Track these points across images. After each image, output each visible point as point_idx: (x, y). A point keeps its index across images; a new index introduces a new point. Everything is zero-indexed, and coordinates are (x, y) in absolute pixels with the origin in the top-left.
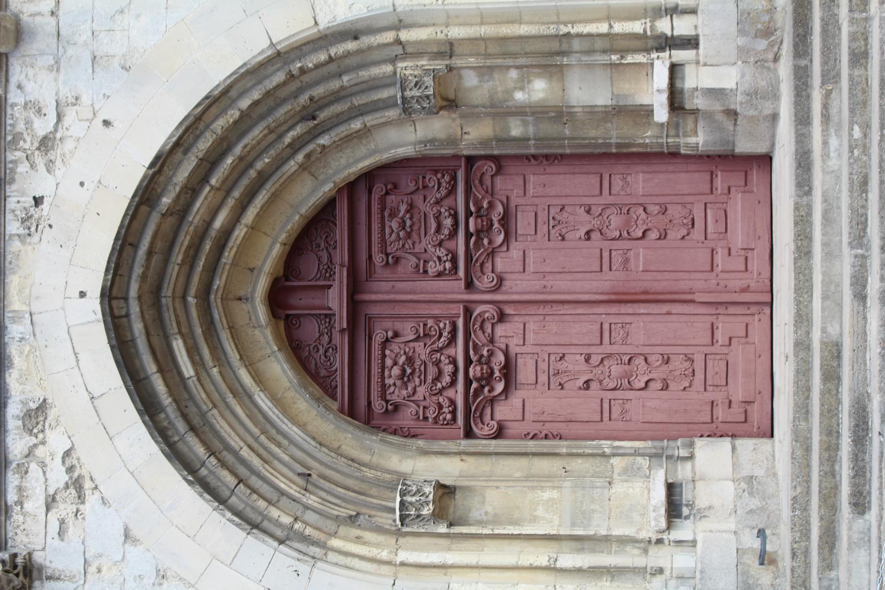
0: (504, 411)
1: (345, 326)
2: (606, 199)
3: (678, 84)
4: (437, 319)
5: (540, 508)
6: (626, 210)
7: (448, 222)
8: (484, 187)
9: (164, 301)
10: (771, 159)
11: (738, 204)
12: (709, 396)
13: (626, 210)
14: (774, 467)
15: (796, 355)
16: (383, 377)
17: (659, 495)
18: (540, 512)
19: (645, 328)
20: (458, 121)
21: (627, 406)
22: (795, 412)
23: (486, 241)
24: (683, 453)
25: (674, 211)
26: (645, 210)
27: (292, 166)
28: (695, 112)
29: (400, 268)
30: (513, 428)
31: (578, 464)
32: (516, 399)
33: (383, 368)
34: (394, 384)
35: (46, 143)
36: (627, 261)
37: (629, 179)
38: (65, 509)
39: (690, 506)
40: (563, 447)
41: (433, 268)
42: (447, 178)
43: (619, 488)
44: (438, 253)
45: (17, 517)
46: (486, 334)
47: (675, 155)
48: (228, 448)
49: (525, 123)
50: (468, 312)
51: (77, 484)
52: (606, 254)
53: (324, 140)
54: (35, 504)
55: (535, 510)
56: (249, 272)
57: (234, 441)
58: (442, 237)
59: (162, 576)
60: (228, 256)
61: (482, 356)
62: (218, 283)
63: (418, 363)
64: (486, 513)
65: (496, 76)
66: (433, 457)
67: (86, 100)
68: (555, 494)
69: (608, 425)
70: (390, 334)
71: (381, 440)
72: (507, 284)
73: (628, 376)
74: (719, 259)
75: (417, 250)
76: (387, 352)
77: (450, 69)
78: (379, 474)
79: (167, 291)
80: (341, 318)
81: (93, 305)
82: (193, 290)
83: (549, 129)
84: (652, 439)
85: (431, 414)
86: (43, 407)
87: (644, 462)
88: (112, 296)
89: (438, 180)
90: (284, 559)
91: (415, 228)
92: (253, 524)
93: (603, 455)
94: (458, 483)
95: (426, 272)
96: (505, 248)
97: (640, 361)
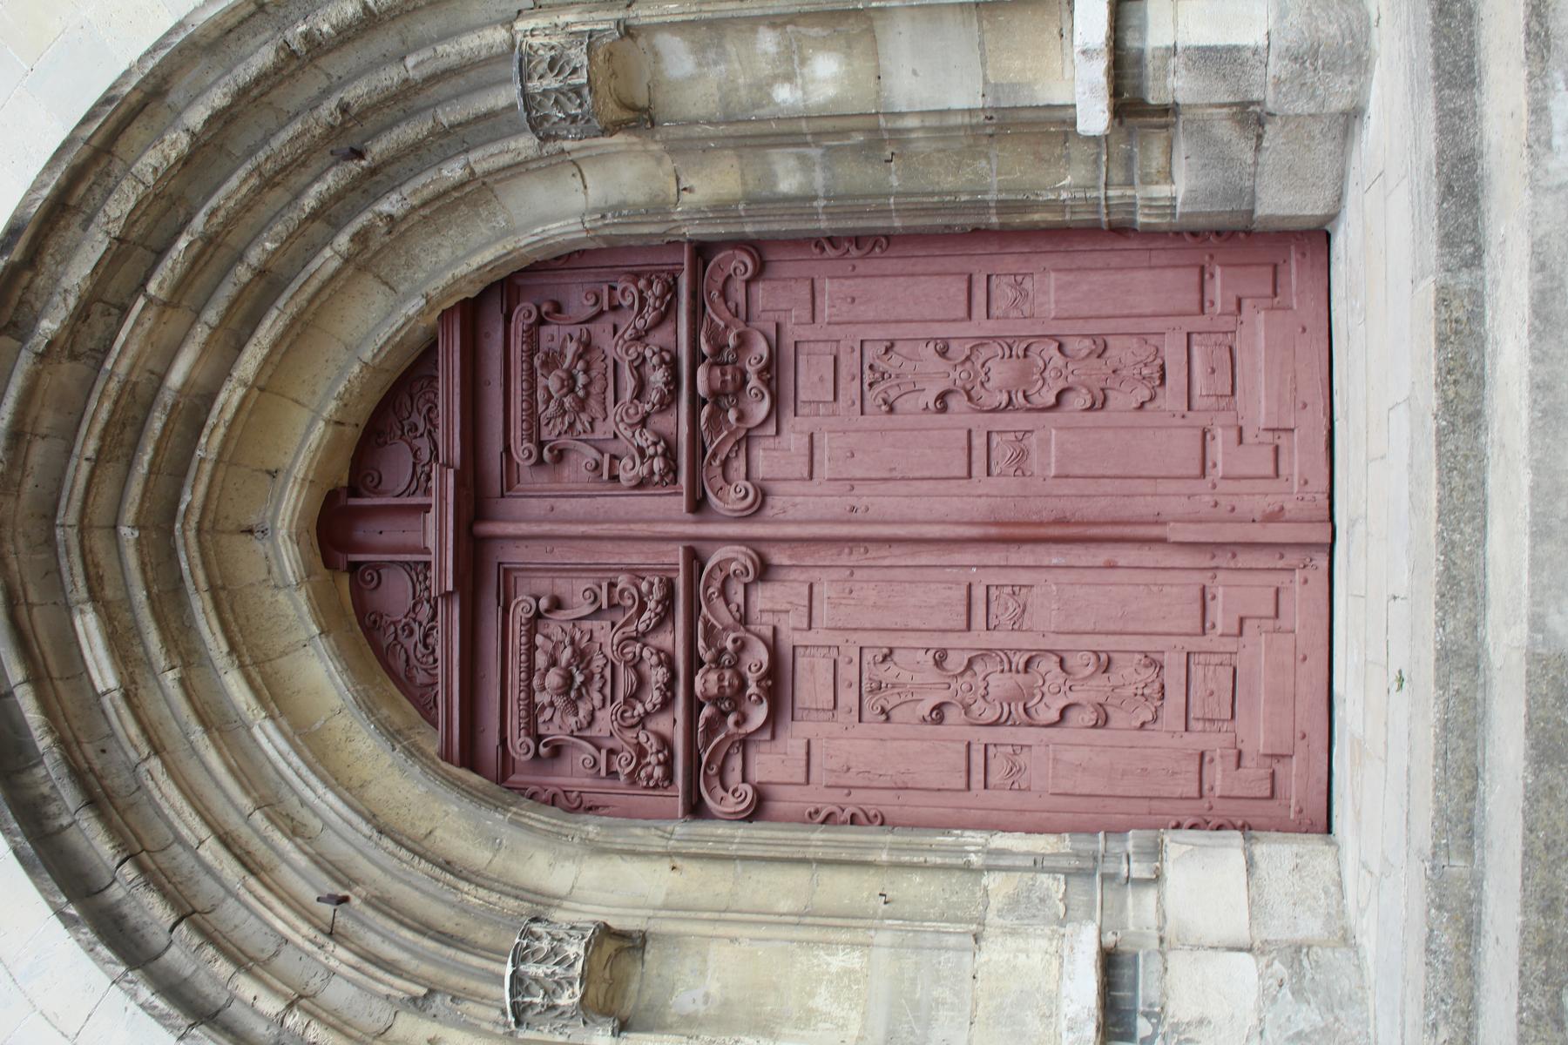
0: (768, 764)
1: (450, 587)
2: (980, 326)
3: (1132, 41)
4: (636, 573)
5: (822, 989)
6: (1021, 348)
7: (657, 377)
8: (731, 305)
9: (59, 532)
10: (1328, 236)
11: (1258, 335)
12: (1195, 741)
13: (1021, 348)
14: (1342, 913)
15: (1442, 684)
16: (530, 692)
18: (822, 1000)
19: (1064, 599)
20: (668, 164)
21: (1022, 759)
22: (1438, 833)
23: (732, 415)
24: (1139, 870)
25: (1120, 350)
26: (1060, 348)
27: (327, 260)
28: (1169, 110)
29: (567, 471)
30: (786, 800)
31: (913, 888)
32: (793, 738)
33: (531, 670)
34: (552, 704)
36: (1022, 455)
37: (1027, 284)
39: (1155, 1016)
40: (881, 846)
41: (629, 471)
42: (657, 288)
43: (995, 952)
44: (639, 440)
46: (733, 607)
47: (1121, 231)
49: (805, 164)
50: (695, 559)
52: (979, 442)
53: (390, 205)
55: (812, 995)
56: (268, 478)
58: (647, 407)
60: (209, 445)
61: (723, 651)
62: (192, 498)
63: (598, 662)
64: (707, 996)
65: (731, 48)
66: (617, 860)
68: (854, 960)
69: (979, 800)
70: (544, 603)
71: (511, 822)
72: (776, 504)
73: (1024, 697)
74: (1217, 451)
75: (598, 435)
76: (539, 639)
77: (628, 31)
78: (494, 897)
79: (69, 515)
80: (442, 570)
82: (130, 513)
83: (857, 176)
84: (1075, 830)
85: (623, 766)
87: (1054, 886)
89: (641, 292)
91: (596, 389)
93: (967, 868)
94: (653, 927)
95: (614, 478)
96: (771, 429)
97: (1049, 665)
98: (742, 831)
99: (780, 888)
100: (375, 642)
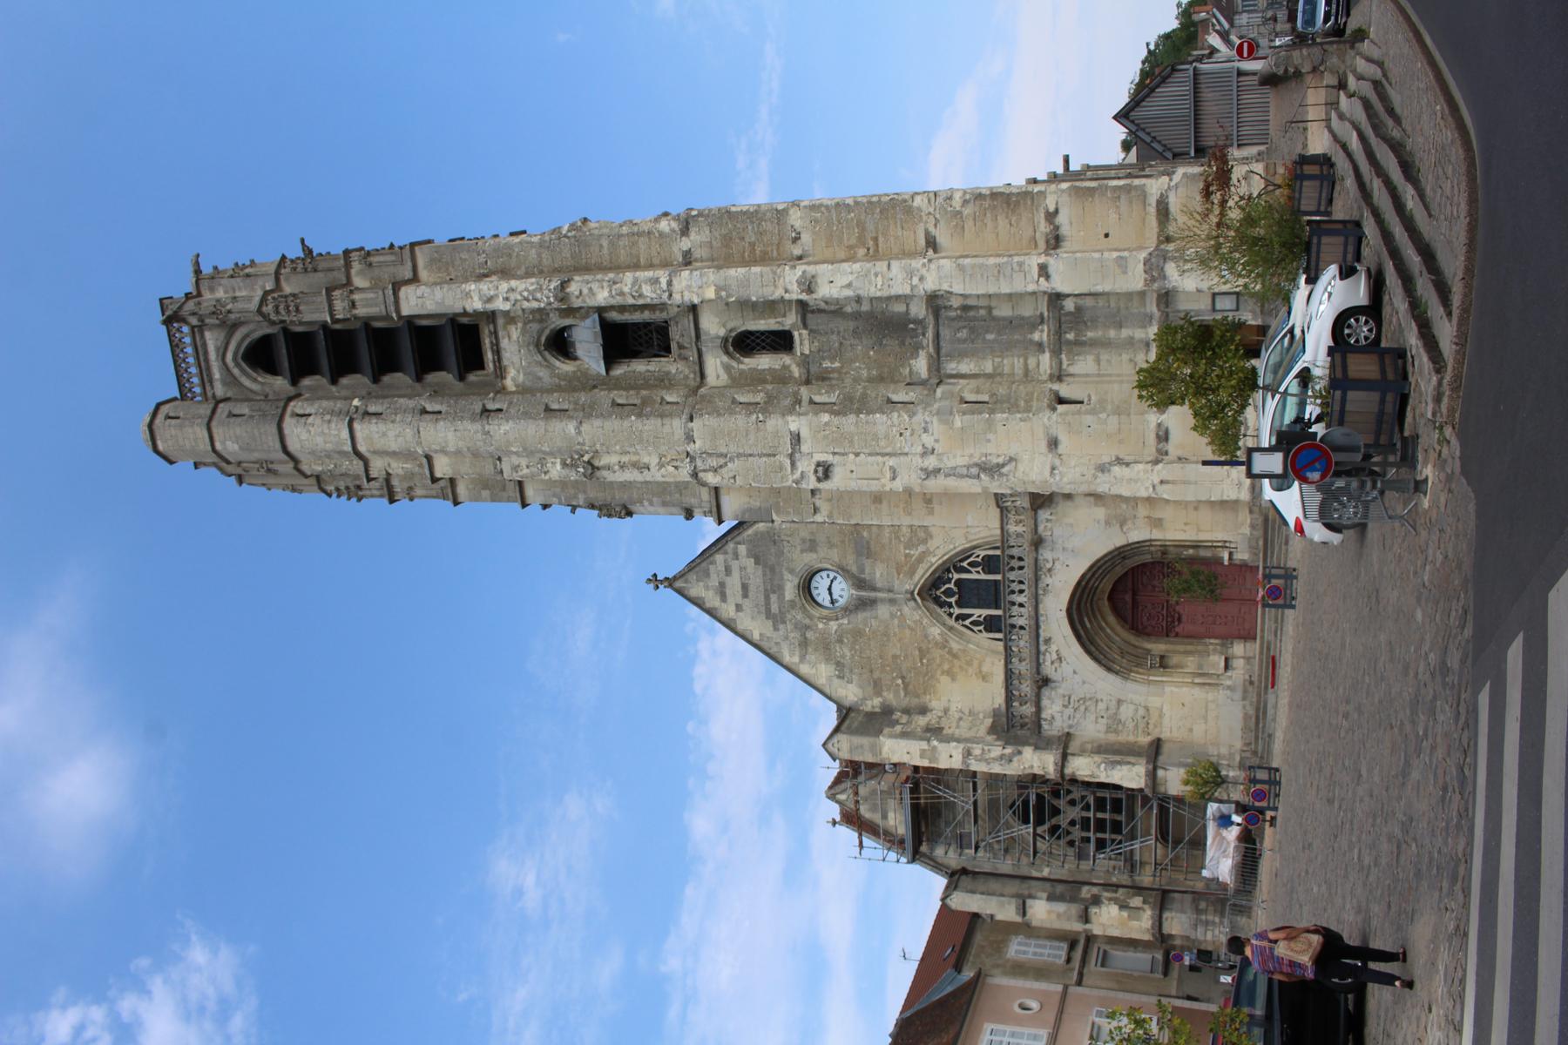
51: (1060, 659)
54: (1048, 663)
81: (1064, 613)
92: (1109, 669)
99: (1181, 648)
100: (1116, 610)
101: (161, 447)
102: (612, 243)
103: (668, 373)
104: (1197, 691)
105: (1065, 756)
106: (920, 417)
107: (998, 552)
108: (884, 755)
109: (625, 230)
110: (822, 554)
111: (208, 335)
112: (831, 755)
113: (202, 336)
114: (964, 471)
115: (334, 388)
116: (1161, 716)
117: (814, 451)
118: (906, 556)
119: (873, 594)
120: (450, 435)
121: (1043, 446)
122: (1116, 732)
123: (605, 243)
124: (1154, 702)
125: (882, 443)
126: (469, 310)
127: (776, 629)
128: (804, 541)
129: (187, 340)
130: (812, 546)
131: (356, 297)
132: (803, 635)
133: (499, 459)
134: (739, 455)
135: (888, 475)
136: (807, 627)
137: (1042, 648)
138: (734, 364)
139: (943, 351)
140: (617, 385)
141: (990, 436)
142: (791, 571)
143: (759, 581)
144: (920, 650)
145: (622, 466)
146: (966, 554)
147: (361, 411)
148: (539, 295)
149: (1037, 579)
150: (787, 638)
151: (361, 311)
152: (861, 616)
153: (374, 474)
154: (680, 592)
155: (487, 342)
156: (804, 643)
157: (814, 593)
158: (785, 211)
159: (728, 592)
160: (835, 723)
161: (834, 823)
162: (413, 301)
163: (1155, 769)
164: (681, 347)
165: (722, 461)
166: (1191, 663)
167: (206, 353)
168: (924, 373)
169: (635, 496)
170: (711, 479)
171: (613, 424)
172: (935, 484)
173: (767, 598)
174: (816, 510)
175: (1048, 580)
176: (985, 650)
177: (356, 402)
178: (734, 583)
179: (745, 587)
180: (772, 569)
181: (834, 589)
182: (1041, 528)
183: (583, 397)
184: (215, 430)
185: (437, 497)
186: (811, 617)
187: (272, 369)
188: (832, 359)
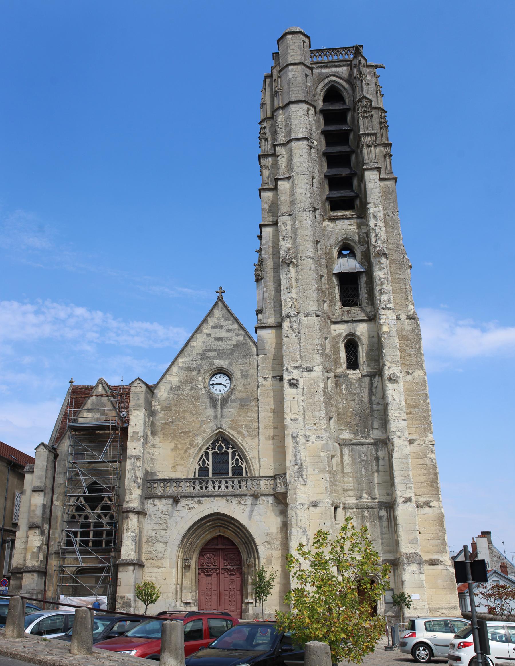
0: (203, 574)
17: (188, 601)
19: (216, 598)
25: (234, 603)
32: (204, 576)
35: (240, 503)
38: (186, 507)
40: (197, 585)
43: (190, 594)
45: (185, 499)
48: (196, 531)
51: (190, 509)
54: (187, 502)
57: (197, 532)
59: (176, 523)
60: (226, 529)
67: (247, 509)
69: (200, 592)
79: (219, 521)
81: (216, 511)
85: (202, 562)
86: (201, 503)
88: (218, 514)
90: (179, 542)
92: (184, 537)
98: (197, 573)
99: (193, 577)
100: (213, 539)
101: (289, 36)
102: (401, 280)
103: (335, 305)
104: (173, 586)
105: (138, 513)
106: (325, 434)
107: (244, 475)
108: (134, 412)
109: (408, 287)
110: (240, 380)
111: (345, 68)
112: (133, 382)
113: (344, 66)
114: (298, 457)
115: (319, 131)
116: (158, 567)
117: (303, 378)
118: (242, 425)
119: (219, 407)
120: (302, 191)
121: (313, 499)
122: (148, 541)
123: (401, 276)
124: (166, 563)
125: (310, 414)
126: (369, 206)
127: (198, 355)
128: (247, 371)
129: (346, 57)
130: (245, 375)
131: (372, 148)
132: (194, 369)
133: (290, 215)
134: (300, 340)
135: (293, 417)
136: (199, 371)
137: (196, 499)
138: (342, 339)
139: (354, 447)
140: (329, 279)
141: (317, 471)
142: (230, 364)
143: (224, 347)
144: (189, 432)
145: (290, 278)
146: (243, 457)
147: (312, 144)
148: (379, 242)
149: (235, 496)
150: (192, 360)
151: (365, 150)
152: (207, 400)
153: (278, 149)
154: (216, 304)
155: (347, 213)
156: (190, 369)
157: (218, 376)
158: (422, 368)
159: (217, 330)
160: (109, 384)
161: (71, 382)
162: (372, 177)
163: (134, 565)
164: (348, 312)
165: (296, 331)
166: (187, 583)
167: (336, 66)
168: (342, 437)
169: (268, 284)
170: (286, 324)
171: (313, 276)
172: (289, 441)
173: (215, 351)
174: (265, 378)
175: (234, 502)
176: (189, 468)
177: (315, 143)
178: (222, 333)
179: (220, 339)
180: (231, 354)
181: (220, 386)
182: (264, 498)
183: (323, 261)
184: (299, 66)
185: (263, 181)
186: (205, 373)
187: (326, 100)
188: (347, 390)
